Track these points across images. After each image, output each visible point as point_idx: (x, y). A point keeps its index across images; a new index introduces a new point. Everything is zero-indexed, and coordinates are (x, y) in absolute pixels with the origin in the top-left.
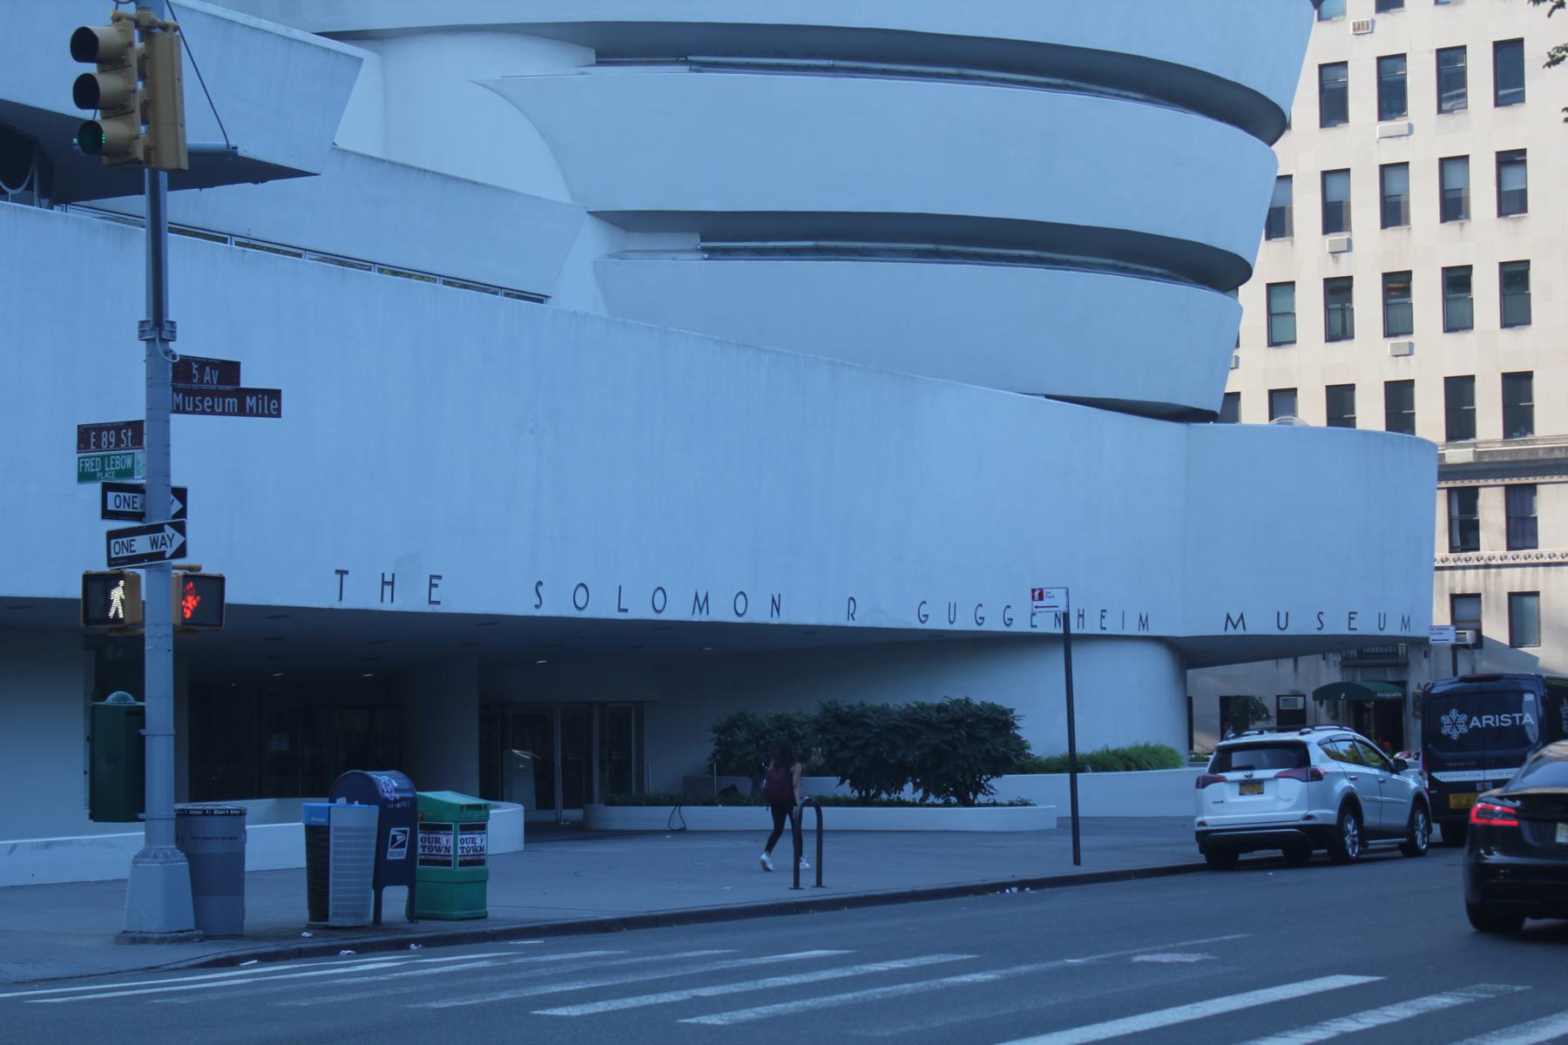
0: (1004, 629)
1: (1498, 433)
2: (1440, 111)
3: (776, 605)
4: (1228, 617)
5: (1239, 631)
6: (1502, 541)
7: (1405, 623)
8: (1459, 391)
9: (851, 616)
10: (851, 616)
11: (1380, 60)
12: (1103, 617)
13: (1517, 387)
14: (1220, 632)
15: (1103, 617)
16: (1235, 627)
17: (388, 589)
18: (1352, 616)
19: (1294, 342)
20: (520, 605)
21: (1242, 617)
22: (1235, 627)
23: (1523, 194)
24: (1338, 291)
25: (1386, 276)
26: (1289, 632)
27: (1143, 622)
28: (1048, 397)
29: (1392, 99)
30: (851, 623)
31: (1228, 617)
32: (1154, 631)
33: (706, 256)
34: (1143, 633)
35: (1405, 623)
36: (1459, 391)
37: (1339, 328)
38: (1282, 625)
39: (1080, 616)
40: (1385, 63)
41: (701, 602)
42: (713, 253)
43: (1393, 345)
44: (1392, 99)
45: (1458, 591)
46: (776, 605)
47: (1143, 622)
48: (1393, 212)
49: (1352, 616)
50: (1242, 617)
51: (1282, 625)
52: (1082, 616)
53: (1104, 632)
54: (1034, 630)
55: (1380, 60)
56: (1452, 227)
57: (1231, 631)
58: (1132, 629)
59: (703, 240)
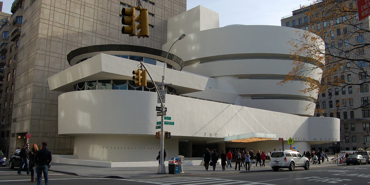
13: (352, 113)
14: (314, 140)
17: (211, 135)
23: (352, 91)
24: (331, 102)
27: (304, 139)
32: (305, 141)
34: (304, 141)
37: (331, 106)
42: (253, 99)
47: (304, 139)
58: (302, 140)
59: (251, 97)
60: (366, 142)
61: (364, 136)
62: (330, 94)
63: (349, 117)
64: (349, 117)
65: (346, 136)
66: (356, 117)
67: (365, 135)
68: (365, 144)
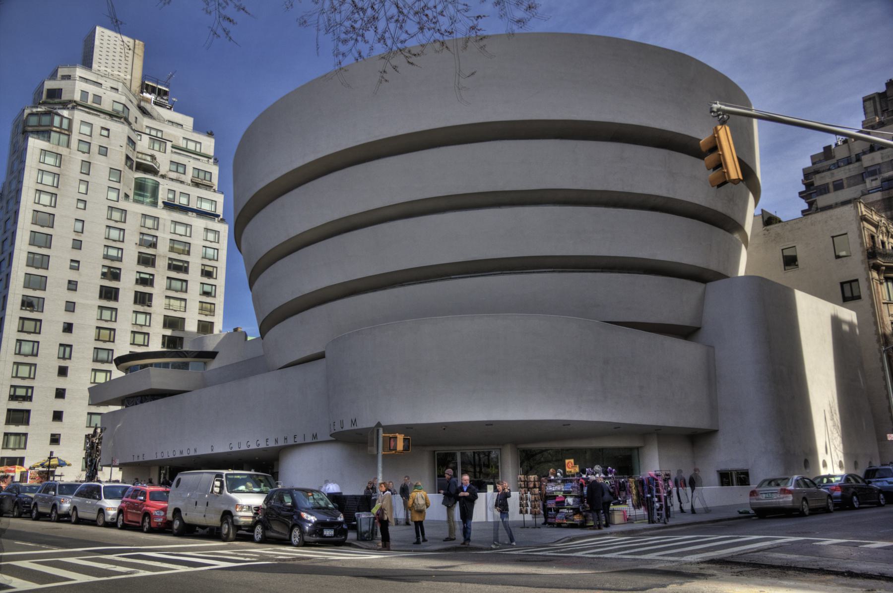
0: (257, 447)
3: (195, 451)
9: (212, 450)
10: (212, 450)
12: (295, 438)
20: (154, 458)
27: (315, 436)
30: (212, 452)
32: (319, 439)
34: (316, 440)
39: (285, 439)
41: (181, 452)
46: (195, 451)
47: (315, 436)
53: (296, 443)
54: (268, 446)
58: (309, 439)
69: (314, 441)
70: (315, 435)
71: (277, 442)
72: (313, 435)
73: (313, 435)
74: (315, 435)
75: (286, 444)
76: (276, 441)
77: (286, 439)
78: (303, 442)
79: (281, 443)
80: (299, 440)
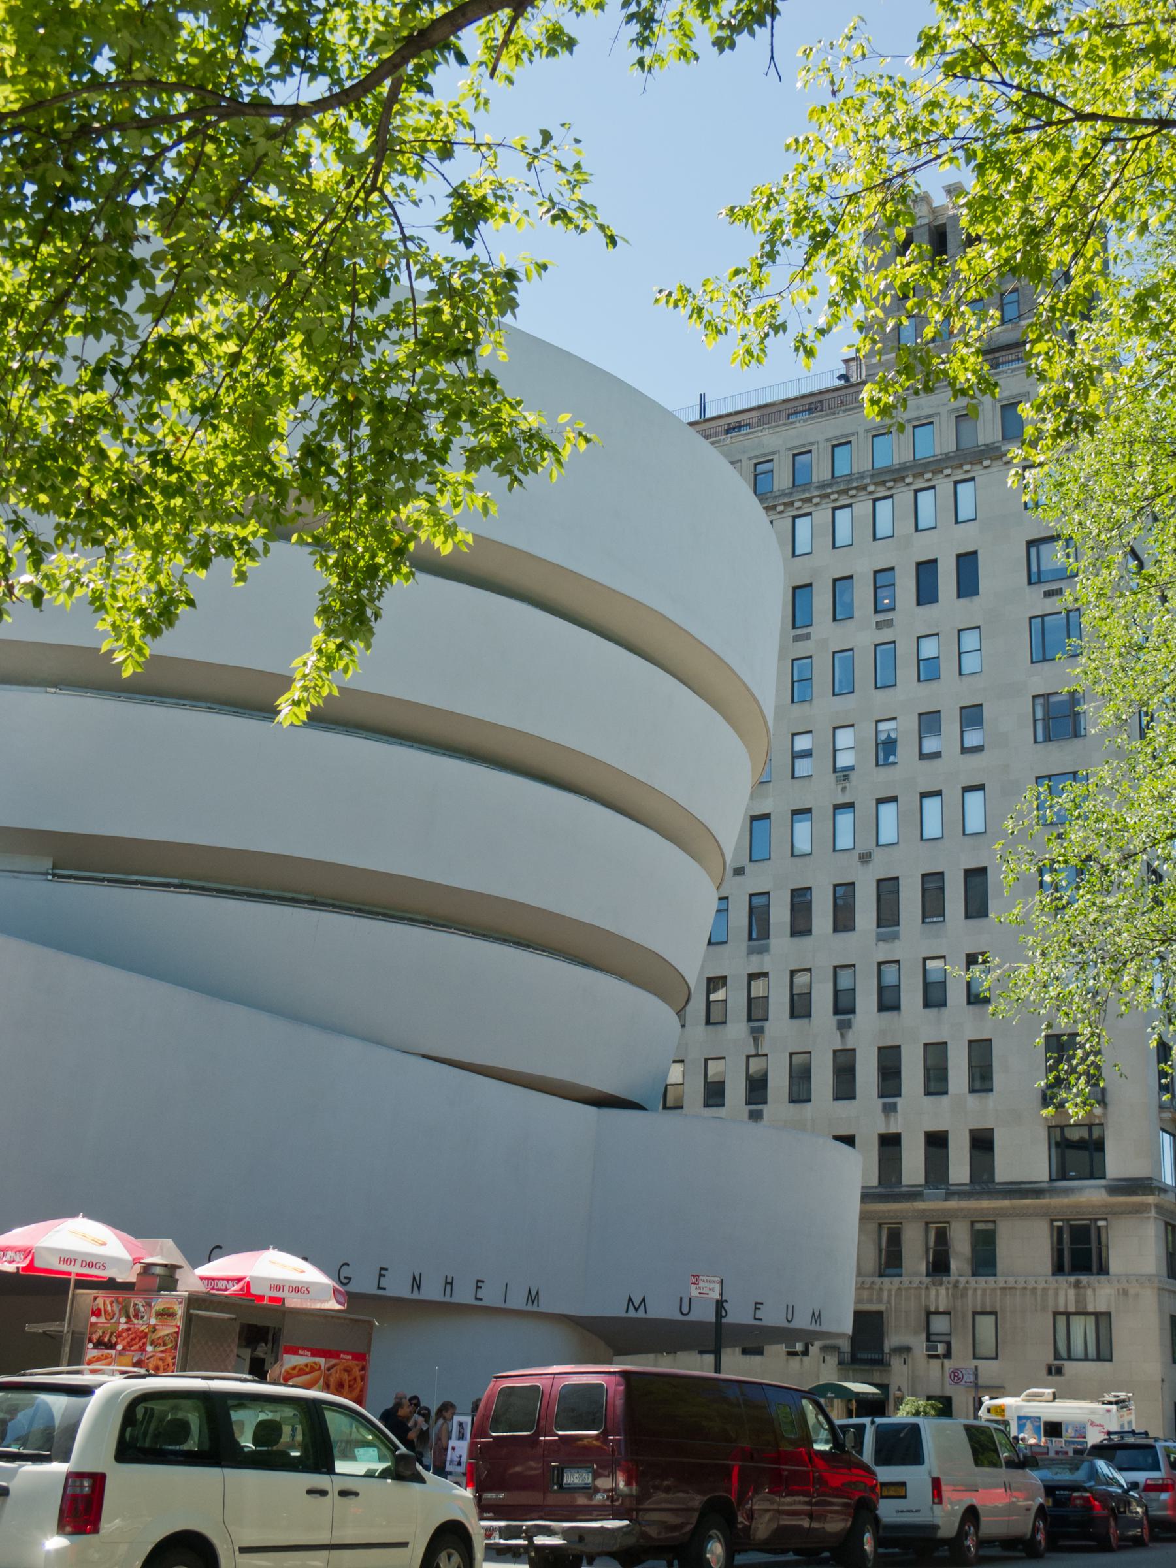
1: (966, 1178)
2: (923, 922)
4: (630, 1300)
5: (641, 1314)
6: (967, 1268)
7: (816, 1317)
8: (937, 1141)
11: (879, 881)
13: (982, 1143)
14: (621, 1313)
15: (478, 1287)
16: (636, 1309)
18: (757, 1306)
19: (809, 1100)
21: (644, 1300)
22: (636, 1309)
25: (880, 1049)
26: (692, 1317)
27: (533, 1297)
28: (425, 1056)
29: (887, 916)
31: (630, 1300)
32: (544, 1308)
33: (50, 877)
34: (535, 1308)
35: (816, 1317)
36: (937, 1141)
38: (685, 1310)
39: (447, 1283)
40: (883, 884)
43: (884, 1105)
44: (887, 916)
45: (933, 1309)
47: (533, 1297)
48: (888, 1002)
49: (757, 1306)
50: (644, 1300)
51: (685, 1310)
52: (451, 1284)
55: (879, 881)
56: (932, 1012)
57: (632, 1313)
58: (517, 1301)
60: (1069, 1358)
61: (1056, 1314)
62: (844, 1006)
63: (959, 1170)
64: (959, 1170)
65: (937, 1313)
66: (1005, 1169)
67: (1062, 1309)
68: (1059, 1371)
69: (530, 1308)
70: (533, 1294)
71: (419, 1288)
72: (530, 1292)
73: (530, 1292)
74: (533, 1294)
75: (447, 1299)
76: (416, 1283)
77: (449, 1283)
78: (502, 1305)
79: (398, 1287)
80: (491, 1297)
